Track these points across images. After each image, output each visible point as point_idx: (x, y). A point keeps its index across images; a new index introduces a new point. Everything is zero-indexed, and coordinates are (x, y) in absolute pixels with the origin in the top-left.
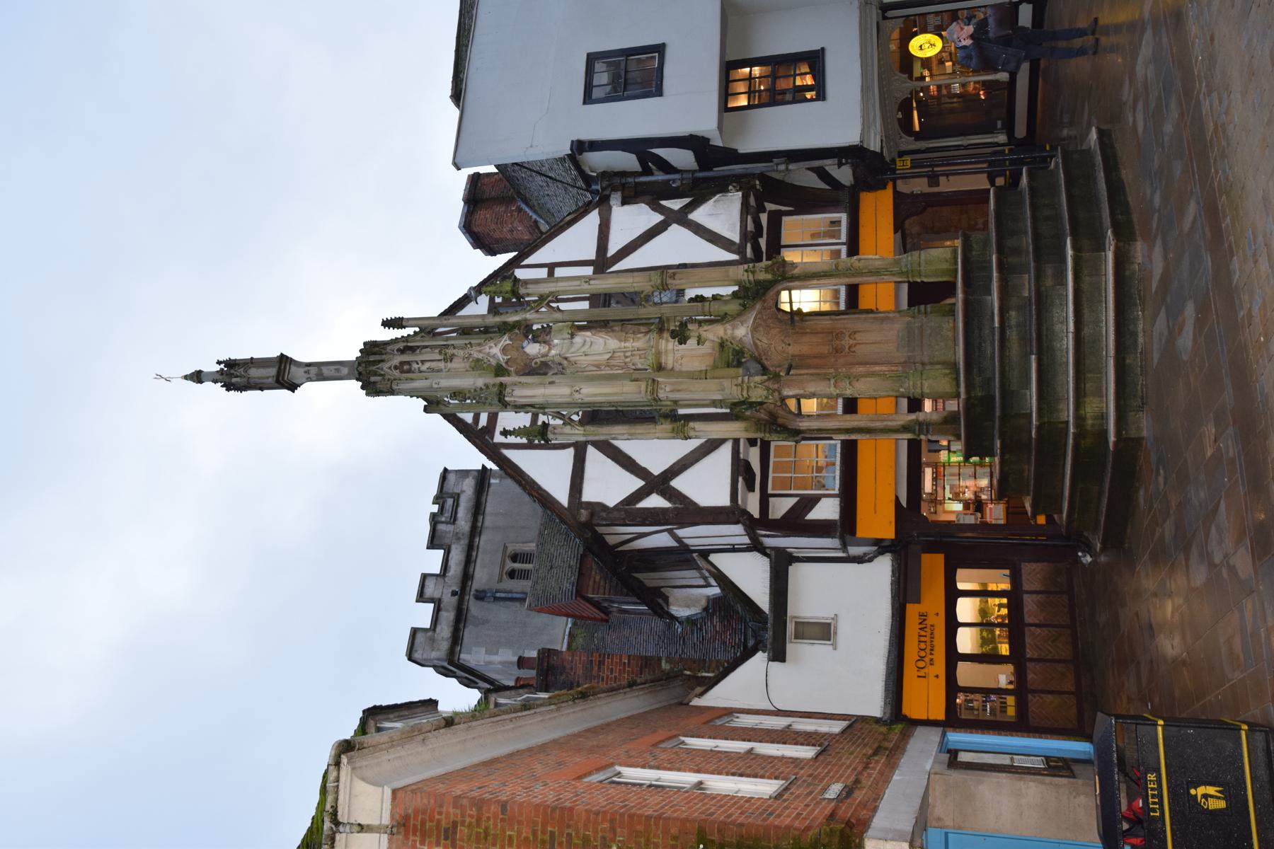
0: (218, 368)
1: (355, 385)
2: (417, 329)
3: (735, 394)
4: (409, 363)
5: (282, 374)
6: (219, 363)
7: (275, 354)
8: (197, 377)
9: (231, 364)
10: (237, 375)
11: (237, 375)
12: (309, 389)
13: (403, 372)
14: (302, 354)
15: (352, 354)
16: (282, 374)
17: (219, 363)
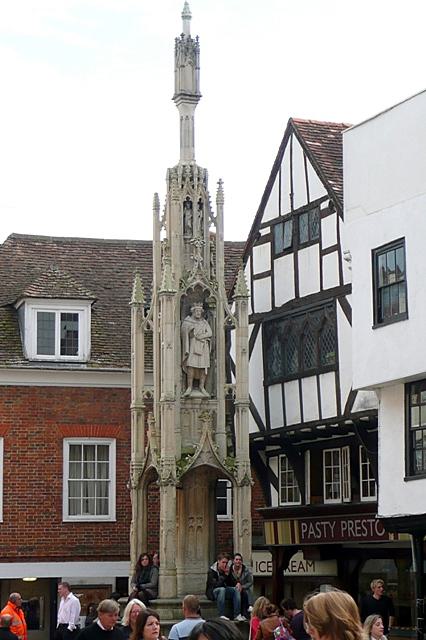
0: (193, 37)
1: (174, 159)
2: (215, 215)
3: (164, 474)
4: (191, 207)
5: (188, 96)
6: (197, 37)
7: (202, 90)
8: (186, 17)
9: (195, 52)
10: (187, 50)
11: (187, 50)
12: (173, 113)
13: (185, 203)
14: (201, 111)
15: (201, 161)
16: (188, 96)
17: (197, 37)
